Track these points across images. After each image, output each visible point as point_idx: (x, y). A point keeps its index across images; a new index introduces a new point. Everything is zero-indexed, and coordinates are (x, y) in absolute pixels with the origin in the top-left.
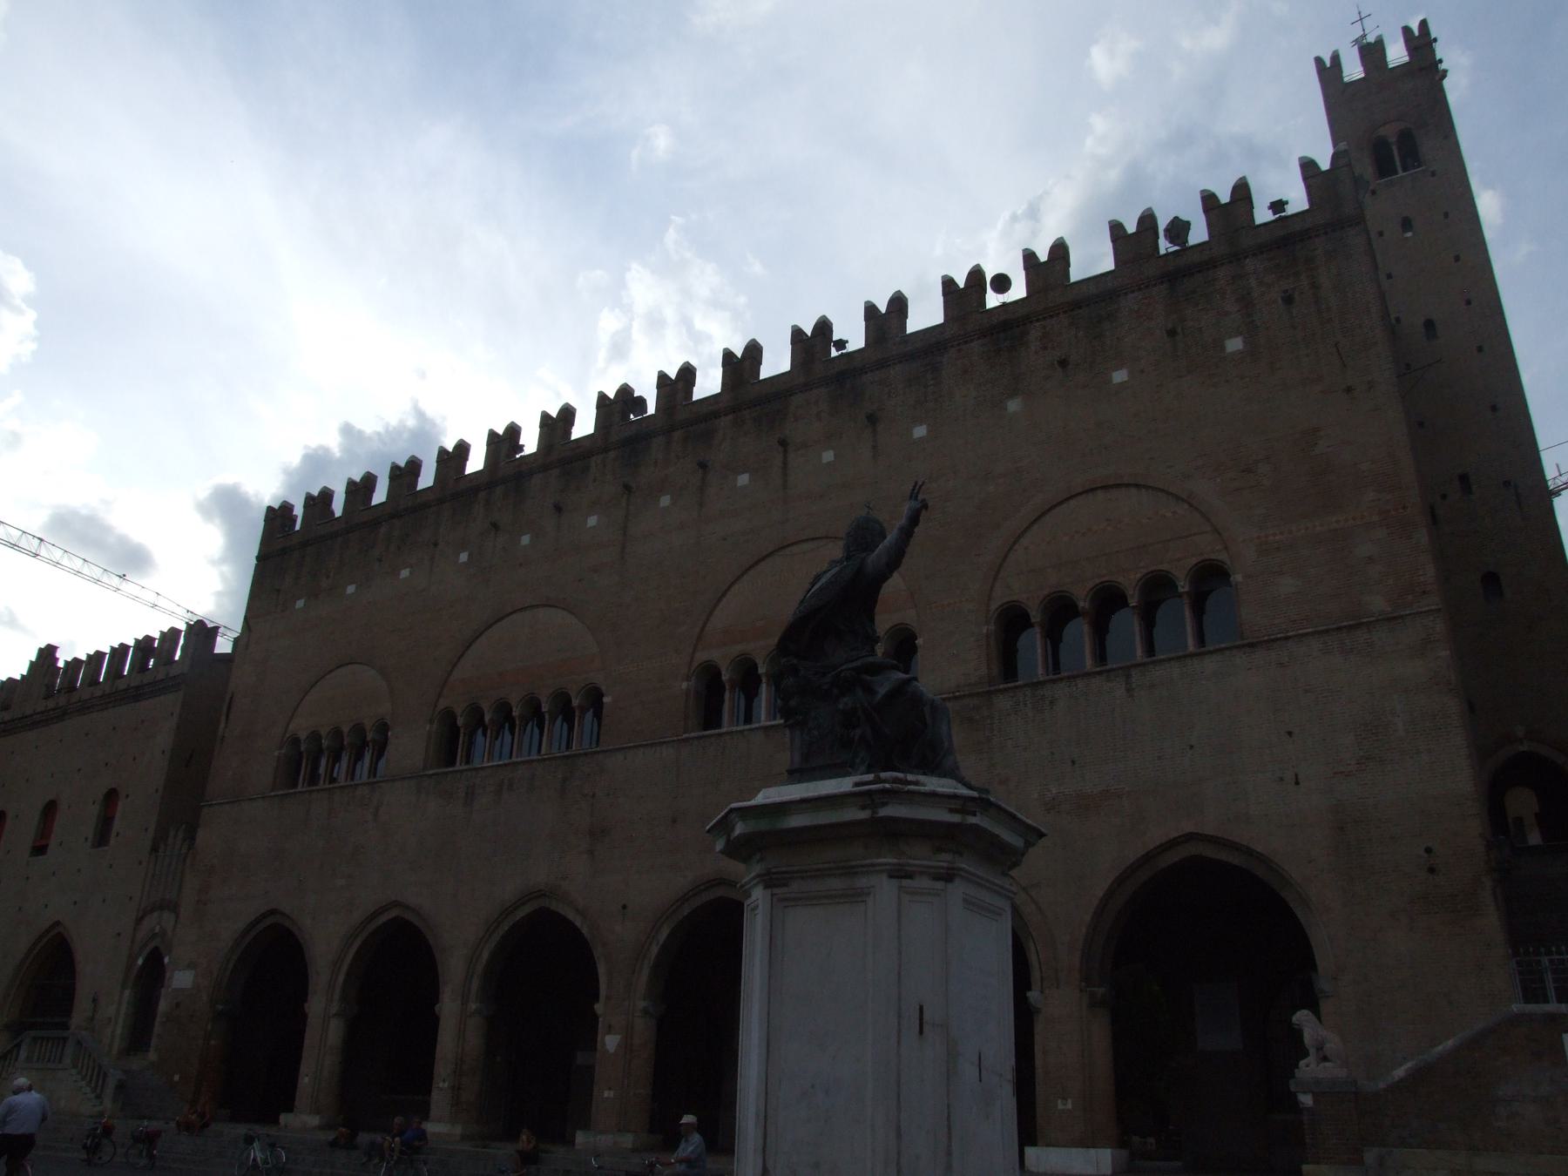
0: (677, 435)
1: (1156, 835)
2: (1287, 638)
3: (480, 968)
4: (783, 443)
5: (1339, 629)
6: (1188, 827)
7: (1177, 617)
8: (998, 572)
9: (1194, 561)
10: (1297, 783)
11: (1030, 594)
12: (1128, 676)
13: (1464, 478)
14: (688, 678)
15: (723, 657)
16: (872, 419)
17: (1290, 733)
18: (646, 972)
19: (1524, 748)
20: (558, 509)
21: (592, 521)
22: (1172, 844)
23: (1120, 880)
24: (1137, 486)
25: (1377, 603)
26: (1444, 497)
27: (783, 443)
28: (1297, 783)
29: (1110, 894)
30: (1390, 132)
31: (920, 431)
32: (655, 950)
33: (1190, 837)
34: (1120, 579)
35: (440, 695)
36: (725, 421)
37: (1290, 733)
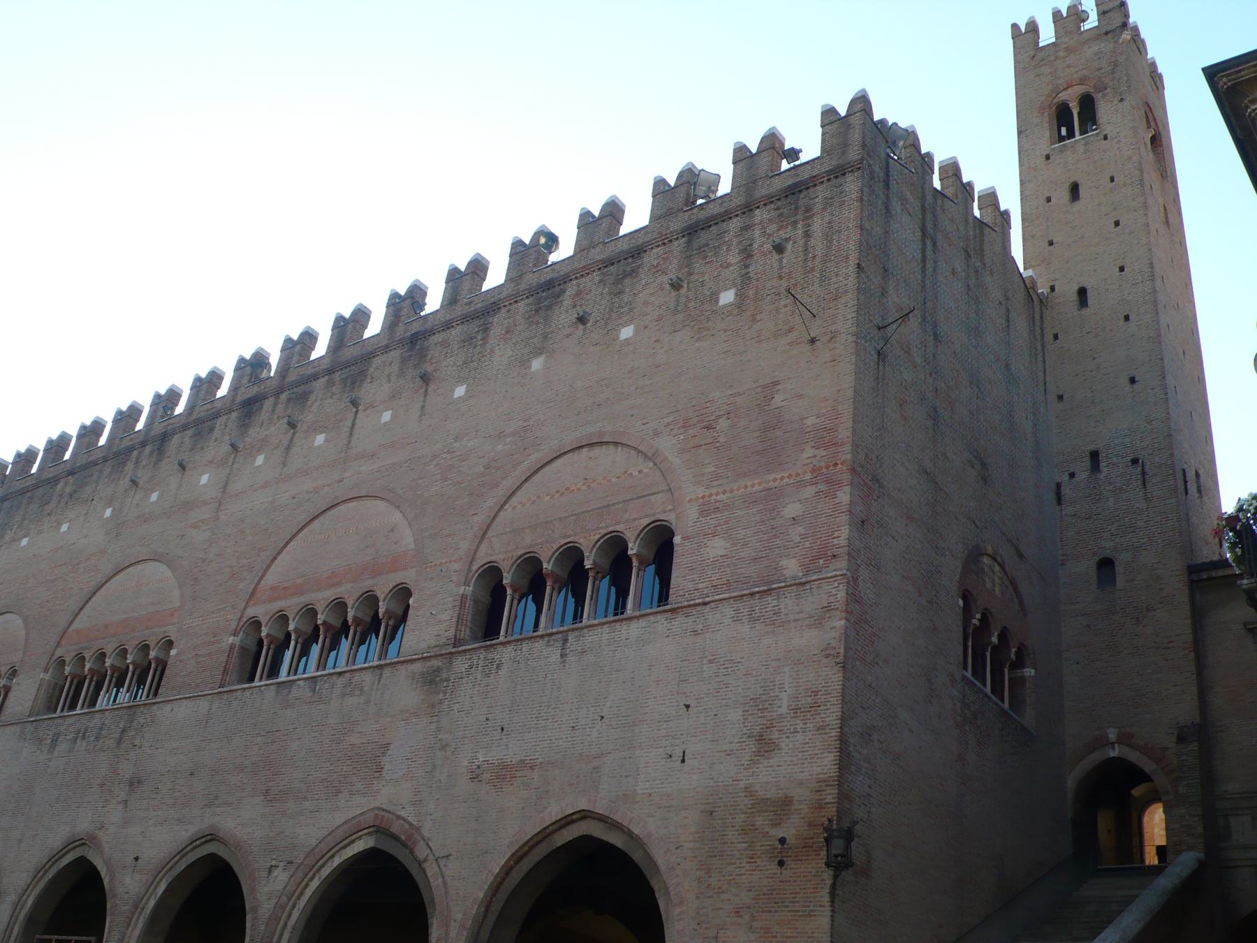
0: (284, 396)
1: (555, 811)
2: (705, 604)
3: (21, 917)
4: (354, 403)
5: (752, 594)
6: (583, 805)
7: (641, 581)
8: (485, 534)
9: (646, 521)
10: (683, 761)
11: (503, 552)
12: (566, 640)
13: (1094, 455)
14: (235, 634)
15: (260, 611)
16: (425, 379)
17: (687, 707)
18: (140, 925)
19: (1115, 753)
20: (182, 467)
21: (204, 479)
22: (566, 821)
23: (518, 857)
24: (616, 444)
25: (791, 567)
26: (1072, 475)
27: (354, 403)
28: (683, 761)
29: (507, 871)
30: (1071, 97)
31: (460, 391)
32: (152, 903)
33: (584, 815)
34: (582, 540)
35: (59, 644)
36: (322, 380)
37: (687, 707)
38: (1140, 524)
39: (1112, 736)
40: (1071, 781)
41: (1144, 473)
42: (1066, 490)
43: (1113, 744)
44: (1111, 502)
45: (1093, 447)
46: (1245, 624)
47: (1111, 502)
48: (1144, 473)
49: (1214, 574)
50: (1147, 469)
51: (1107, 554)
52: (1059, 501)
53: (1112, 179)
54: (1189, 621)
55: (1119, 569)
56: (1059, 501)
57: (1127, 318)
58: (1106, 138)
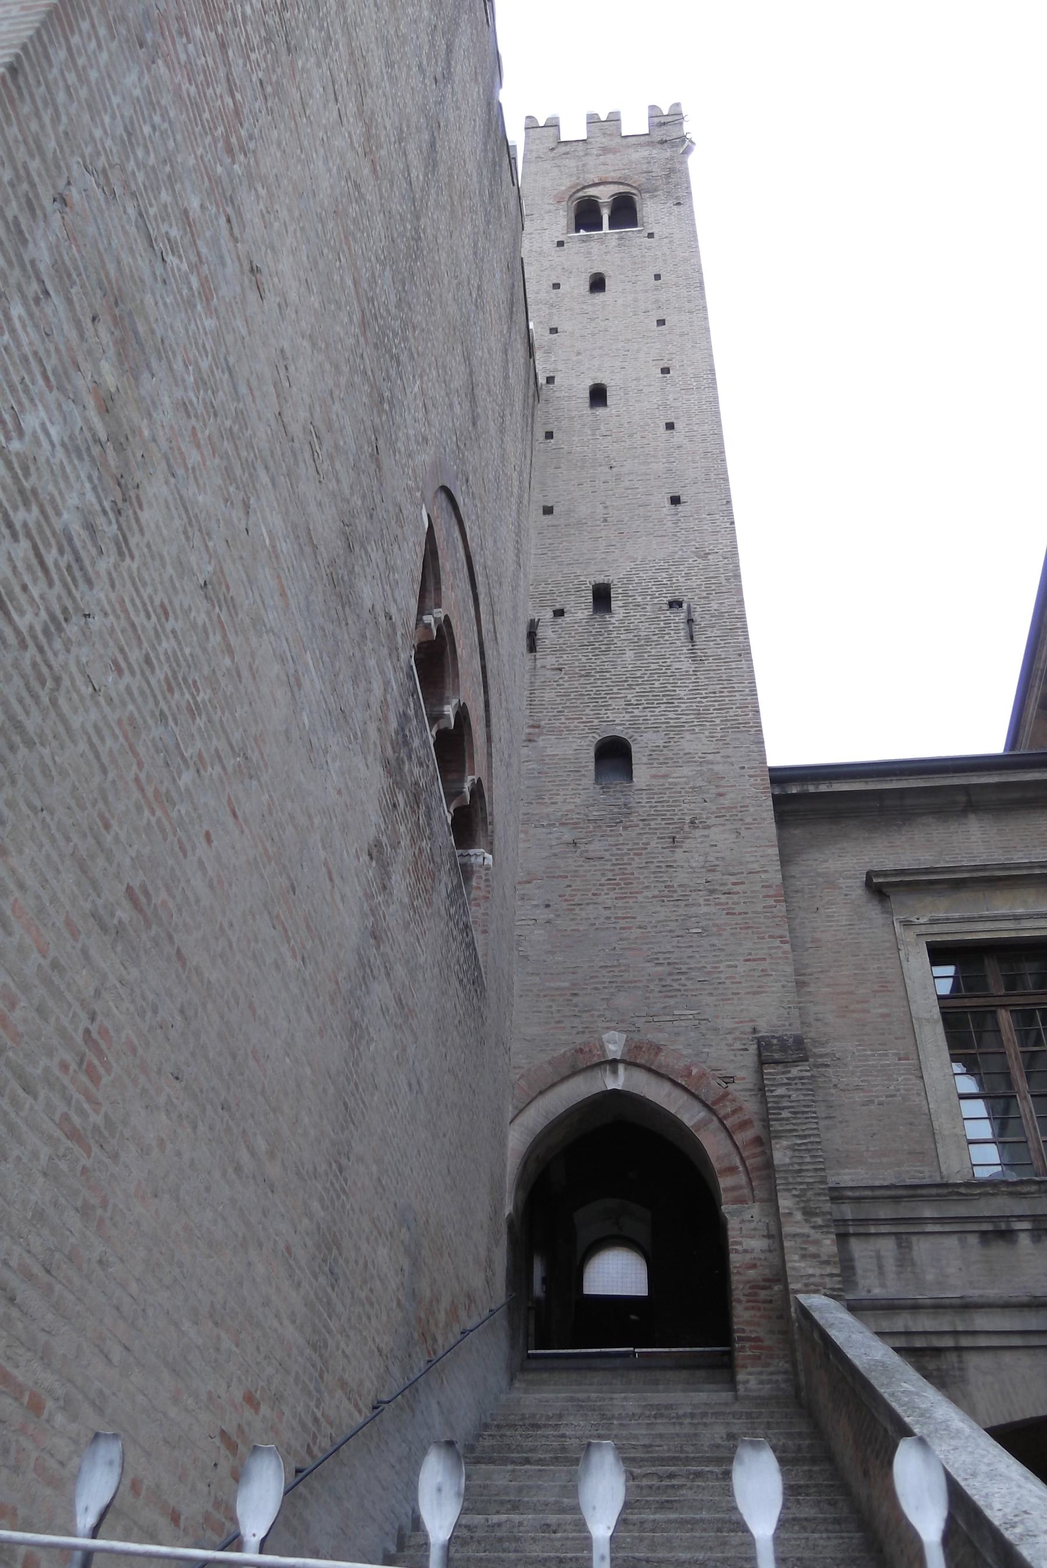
19: (617, 1081)
30: (604, 195)
38: (681, 693)
39: (614, 1046)
40: (517, 1139)
41: (690, 621)
42: (546, 634)
43: (614, 1063)
44: (629, 655)
45: (601, 579)
46: (870, 875)
47: (629, 655)
48: (690, 621)
49: (812, 789)
50: (696, 616)
51: (619, 731)
52: (532, 647)
53: (657, 277)
54: (776, 850)
55: (638, 756)
56: (532, 647)
57: (670, 426)
58: (651, 235)
